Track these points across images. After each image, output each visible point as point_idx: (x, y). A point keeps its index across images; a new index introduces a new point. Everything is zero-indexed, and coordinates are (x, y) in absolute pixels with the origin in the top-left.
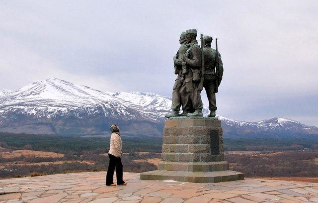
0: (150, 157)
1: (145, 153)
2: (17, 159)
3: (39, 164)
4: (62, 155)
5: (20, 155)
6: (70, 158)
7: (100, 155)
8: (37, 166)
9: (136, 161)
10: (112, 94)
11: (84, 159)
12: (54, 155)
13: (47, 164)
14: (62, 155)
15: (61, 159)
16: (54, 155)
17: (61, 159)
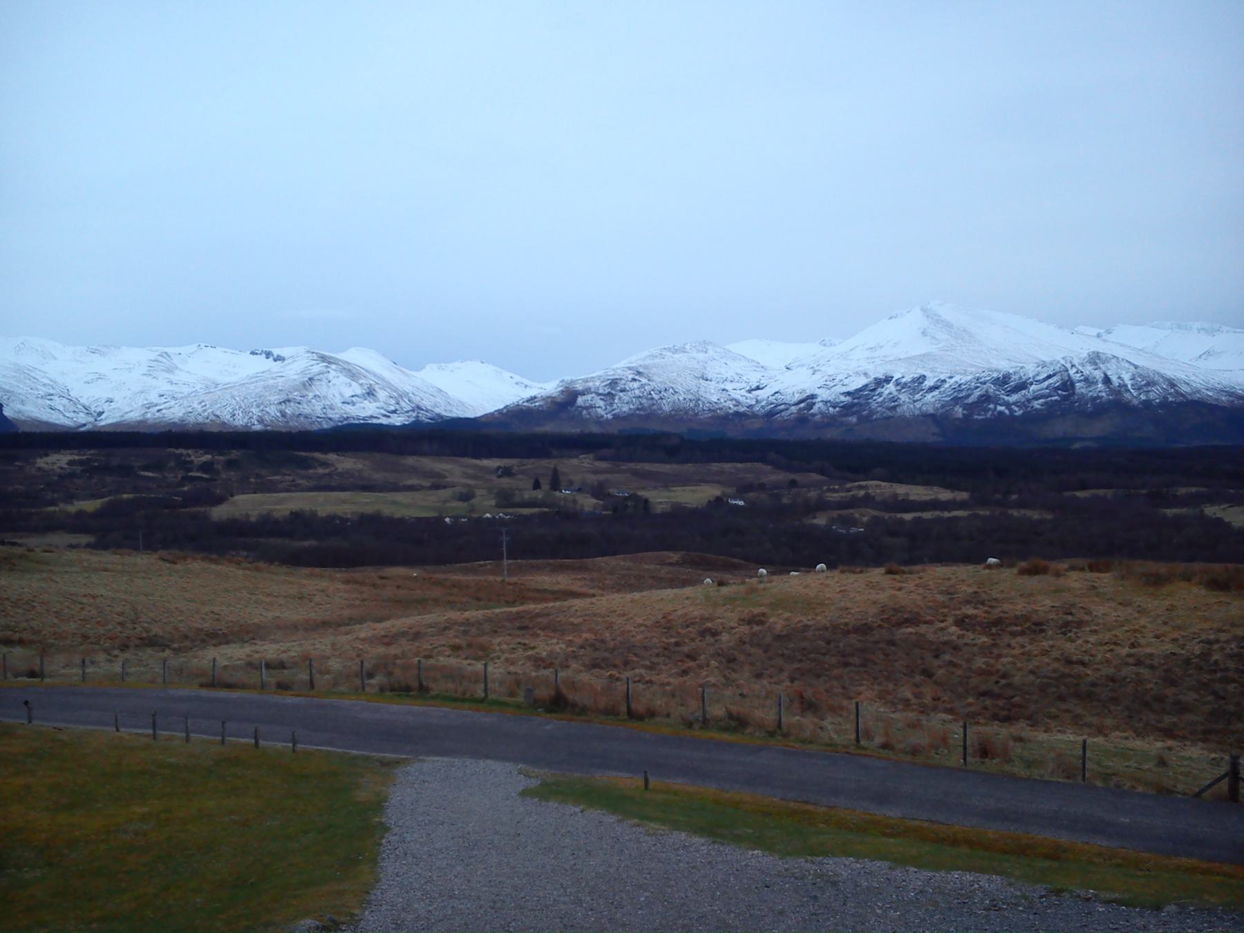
0: (1212, 499)
1: (1193, 490)
2: (853, 503)
3: (908, 517)
4: (964, 496)
5: (862, 493)
6: (984, 503)
7: (1067, 494)
8: (902, 521)
9: (1170, 512)
10: (1095, 332)
11: (1020, 505)
12: (945, 495)
13: (927, 515)
14: (964, 496)
15: (962, 505)
16: (945, 495)
17: (962, 505)
